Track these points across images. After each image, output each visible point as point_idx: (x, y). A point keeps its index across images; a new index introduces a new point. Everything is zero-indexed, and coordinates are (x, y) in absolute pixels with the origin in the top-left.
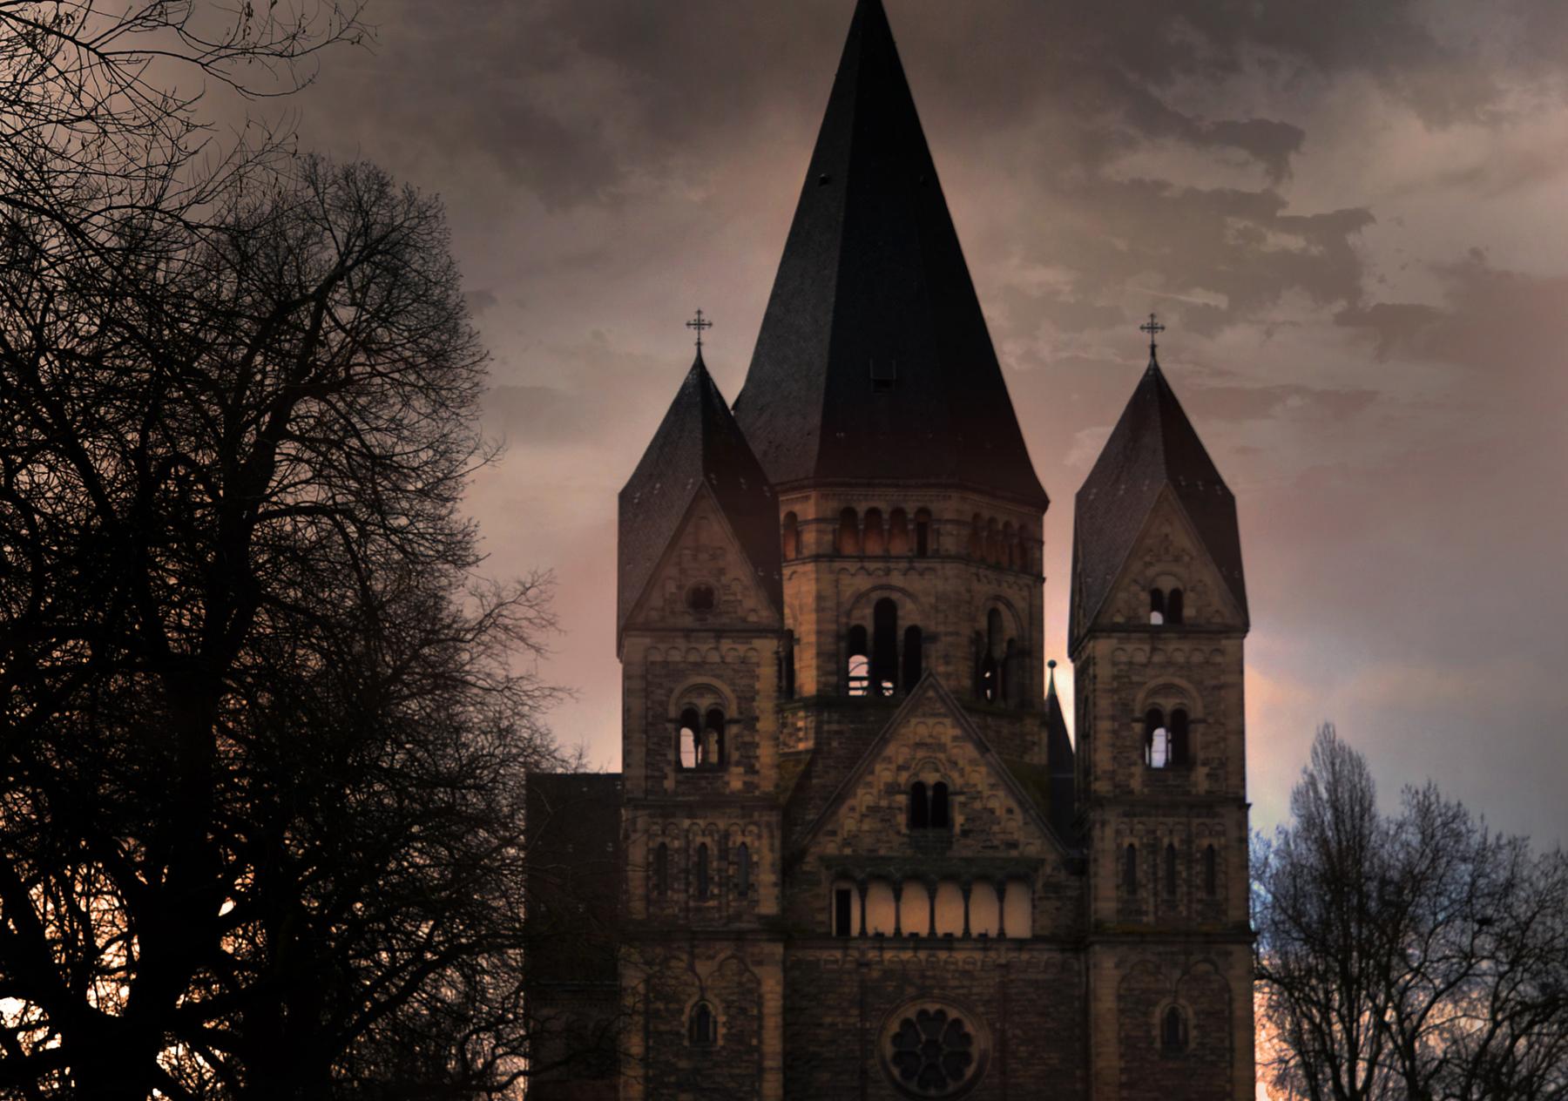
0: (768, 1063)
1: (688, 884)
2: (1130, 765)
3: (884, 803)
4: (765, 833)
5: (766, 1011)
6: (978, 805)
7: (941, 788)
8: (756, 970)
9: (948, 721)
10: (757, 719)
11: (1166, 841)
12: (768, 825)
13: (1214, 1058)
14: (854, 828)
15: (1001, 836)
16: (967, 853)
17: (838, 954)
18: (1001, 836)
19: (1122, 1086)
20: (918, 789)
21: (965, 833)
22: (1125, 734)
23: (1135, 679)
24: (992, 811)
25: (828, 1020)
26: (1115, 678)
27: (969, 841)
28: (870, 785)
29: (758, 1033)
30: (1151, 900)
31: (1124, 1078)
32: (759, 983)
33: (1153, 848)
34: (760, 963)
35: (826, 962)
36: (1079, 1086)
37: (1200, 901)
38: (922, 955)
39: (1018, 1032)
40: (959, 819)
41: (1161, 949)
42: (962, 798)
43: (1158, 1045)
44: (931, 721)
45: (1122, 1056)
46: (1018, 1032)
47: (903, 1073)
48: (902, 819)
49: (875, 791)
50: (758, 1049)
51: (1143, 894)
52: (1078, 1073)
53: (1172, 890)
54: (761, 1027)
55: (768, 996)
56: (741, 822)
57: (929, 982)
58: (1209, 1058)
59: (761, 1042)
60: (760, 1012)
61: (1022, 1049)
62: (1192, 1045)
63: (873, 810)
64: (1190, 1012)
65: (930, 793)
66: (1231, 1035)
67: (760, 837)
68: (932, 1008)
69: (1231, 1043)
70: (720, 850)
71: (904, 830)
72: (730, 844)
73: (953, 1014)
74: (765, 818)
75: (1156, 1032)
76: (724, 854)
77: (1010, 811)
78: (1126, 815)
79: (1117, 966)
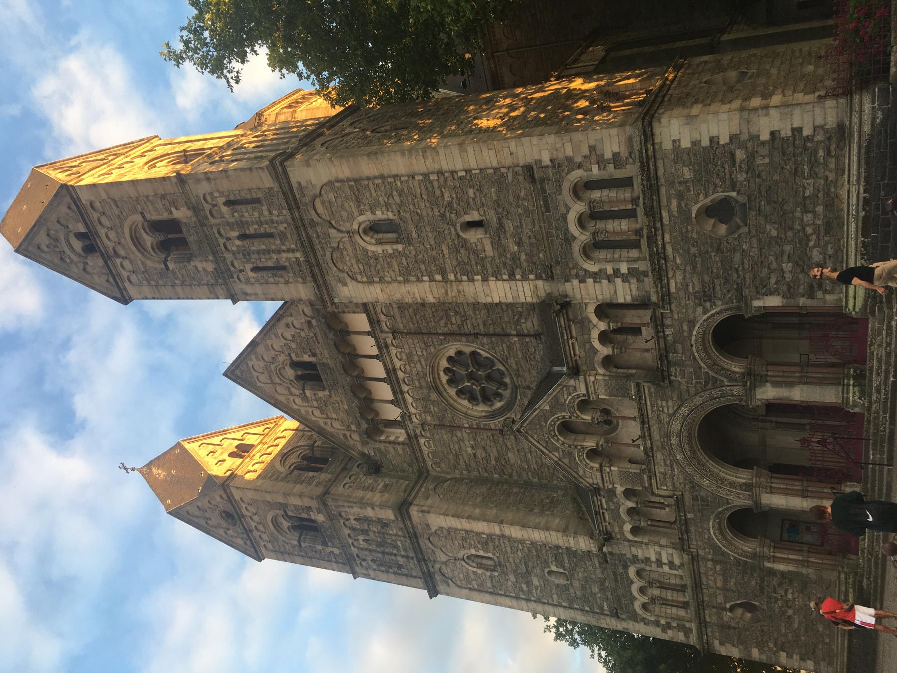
1: (391, 554)
11: (238, 242)
16: (327, 355)
19: (445, 280)
21: (314, 355)
27: (318, 352)
31: (438, 277)
38: (405, 388)
39: (442, 323)
41: (318, 247)
42: (293, 355)
43: (400, 247)
45: (419, 280)
48: (321, 394)
57: (424, 384)
58: (397, 199)
61: (454, 320)
62: (390, 215)
65: (299, 373)
66: (368, 179)
68: (444, 378)
71: (327, 393)
73: (444, 364)
75: (389, 249)
79: (345, 284)
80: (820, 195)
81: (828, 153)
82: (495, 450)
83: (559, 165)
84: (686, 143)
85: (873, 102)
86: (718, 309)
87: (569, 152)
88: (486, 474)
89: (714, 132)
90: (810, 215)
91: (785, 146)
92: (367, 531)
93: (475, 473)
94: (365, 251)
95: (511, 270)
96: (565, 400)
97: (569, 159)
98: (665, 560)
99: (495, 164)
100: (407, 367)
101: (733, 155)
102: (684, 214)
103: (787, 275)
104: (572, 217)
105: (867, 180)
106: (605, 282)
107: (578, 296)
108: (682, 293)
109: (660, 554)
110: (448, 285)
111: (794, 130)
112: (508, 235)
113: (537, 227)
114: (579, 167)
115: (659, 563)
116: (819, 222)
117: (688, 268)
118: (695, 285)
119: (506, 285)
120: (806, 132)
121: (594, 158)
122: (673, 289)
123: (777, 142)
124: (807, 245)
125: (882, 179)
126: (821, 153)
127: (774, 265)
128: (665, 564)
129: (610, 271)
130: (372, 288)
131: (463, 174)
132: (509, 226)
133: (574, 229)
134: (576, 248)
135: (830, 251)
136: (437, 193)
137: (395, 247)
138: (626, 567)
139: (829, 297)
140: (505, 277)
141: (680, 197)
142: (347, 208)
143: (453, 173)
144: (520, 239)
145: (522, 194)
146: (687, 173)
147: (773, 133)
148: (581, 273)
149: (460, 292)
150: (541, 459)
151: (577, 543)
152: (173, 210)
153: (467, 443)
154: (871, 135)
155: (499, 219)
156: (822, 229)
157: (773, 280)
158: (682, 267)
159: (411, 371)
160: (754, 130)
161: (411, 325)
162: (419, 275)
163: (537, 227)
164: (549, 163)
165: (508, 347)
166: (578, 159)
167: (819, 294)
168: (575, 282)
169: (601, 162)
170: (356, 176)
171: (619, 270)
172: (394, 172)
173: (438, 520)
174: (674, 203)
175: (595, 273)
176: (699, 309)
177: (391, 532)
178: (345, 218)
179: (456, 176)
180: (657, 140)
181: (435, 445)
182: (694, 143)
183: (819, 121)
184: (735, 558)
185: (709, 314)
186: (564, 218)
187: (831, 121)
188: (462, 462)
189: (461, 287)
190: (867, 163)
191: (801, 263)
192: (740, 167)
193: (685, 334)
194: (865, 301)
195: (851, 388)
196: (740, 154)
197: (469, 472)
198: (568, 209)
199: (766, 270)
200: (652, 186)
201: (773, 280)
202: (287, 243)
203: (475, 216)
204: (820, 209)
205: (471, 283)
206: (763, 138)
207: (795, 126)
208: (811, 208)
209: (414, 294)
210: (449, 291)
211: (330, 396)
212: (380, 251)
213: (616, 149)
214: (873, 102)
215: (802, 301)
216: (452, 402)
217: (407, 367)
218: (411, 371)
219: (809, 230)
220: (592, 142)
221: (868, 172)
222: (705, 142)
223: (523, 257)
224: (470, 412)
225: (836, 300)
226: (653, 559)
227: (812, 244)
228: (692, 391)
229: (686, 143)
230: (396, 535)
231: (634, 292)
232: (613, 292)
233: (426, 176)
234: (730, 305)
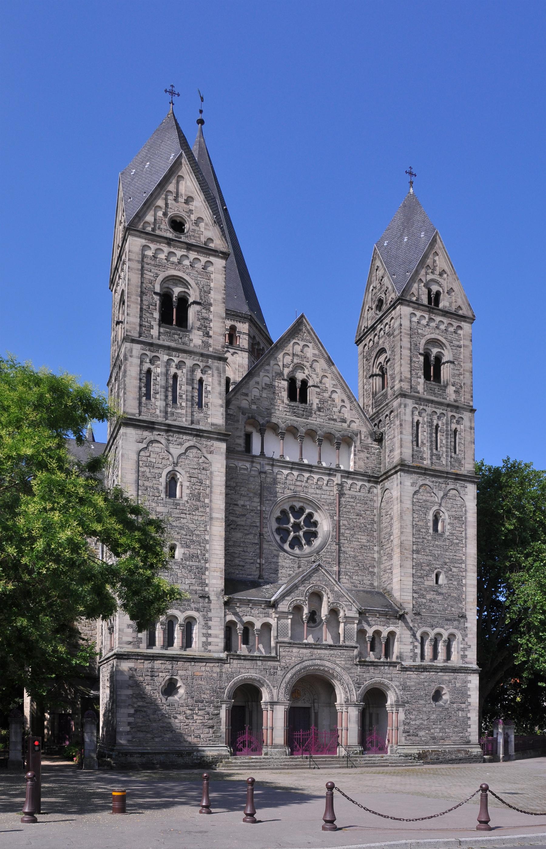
17: (248, 465)
25: (241, 502)
35: (241, 469)
82: (243, 523)
84: (469, 685)
89: (472, 697)
97: (466, 636)
98: (210, 640)
101: (464, 703)
104: (441, 631)
109: (216, 637)
111: (470, 725)
112: (435, 596)
113: (438, 612)
114: (463, 640)
115: (210, 635)
121: (466, 646)
128: (207, 639)
132: (440, 598)
133: (437, 630)
134: (428, 630)
138: (197, 610)
141: (450, 682)
144: (432, 602)
145: (453, 609)
147: (470, 718)
150: (239, 557)
153: (248, 503)
160: (471, 711)
163: (438, 612)
166: (466, 639)
169: (464, 649)
171: (417, 648)
180: (471, 675)
181: (243, 474)
182: (469, 688)
183: (472, 734)
184: (226, 687)
186: (443, 627)
187: (471, 738)
196: (463, 706)
198: (446, 630)
200: (455, 670)
206: (468, 714)
222: (469, 693)
226: (210, 632)
229: (469, 685)
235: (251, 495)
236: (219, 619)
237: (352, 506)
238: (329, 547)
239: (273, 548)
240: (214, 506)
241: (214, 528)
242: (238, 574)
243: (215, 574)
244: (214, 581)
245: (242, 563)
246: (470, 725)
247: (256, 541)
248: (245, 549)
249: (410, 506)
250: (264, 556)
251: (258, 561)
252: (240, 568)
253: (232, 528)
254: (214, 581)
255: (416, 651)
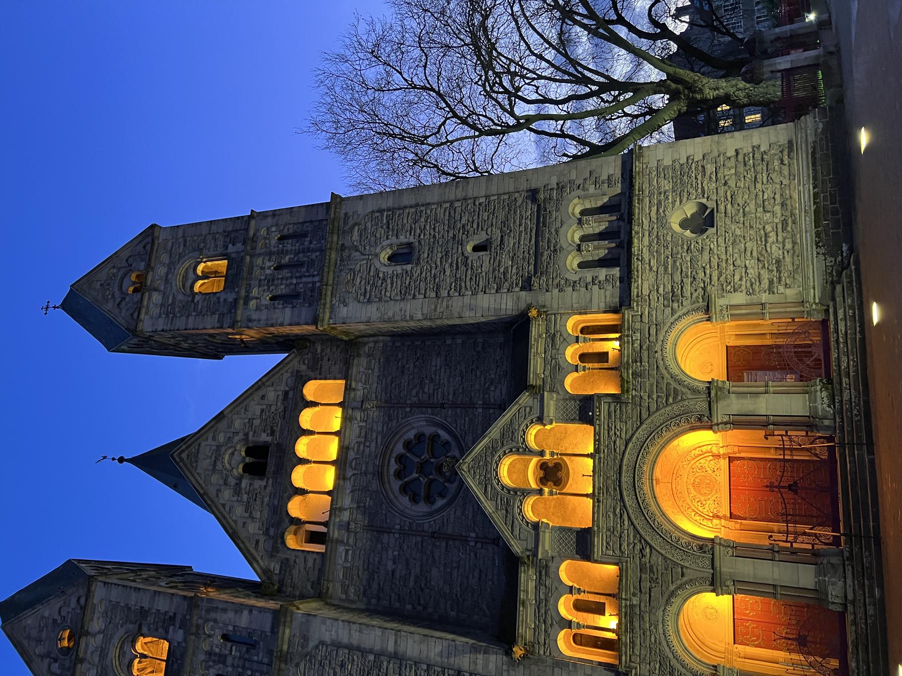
0: (391, 648)
2: (219, 302)
3: (245, 497)
4: (213, 615)
5: (345, 640)
6: (257, 422)
7: (249, 452)
8: (312, 644)
9: (203, 444)
10: (142, 608)
12: (208, 611)
13: (423, 220)
14: (257, 525)
15: (279, 404)
17: (341, 549)
18: (279, 404)
20: (247, 469)
21: (272, 433)
22: (200, 307)
23: (170, 301)
24: (262, 411)
25: (390, 565)
26: (167, 316)
28: (231, 508)
29: (364, 652)
30: (304, 280)
31: (433, 295)
32: (322, 643)
33: (271, 281)
34: (306, 639)
36: (459, 341)
37: (311, 243)
40: (264, 437)
42: (251, 434)
44: (201, 456)
45: (414, 297)
46: (414, 392)
47: (442, 495)
49: (236, 504)
50: (378, 655)
51: (301, 289)
52: (449, 342)
53: (302, 264)
54: (358, 649)
55: (334, 637)
56: (203, 636)
59: (371, 651)
60: (346, 647)
62: (412, 239)
63: (248, 508)
64: (388, 242)
66: (406, 207)
67: (215, 621)
69: (411, 207)
70: (219, 662)
72: (217, 650)
73: (399, 449)
74: (203, 612)
75: (399, 269)
76: (222, 659)
77: (263, 397)
78: (246, 303)
80: (777, 196)
81: (782, 163)
83: (563, 187)
85: (815, 118)
86: (685, 310)
87: (573, 176)
88: (397, 605)
89: (690, 151)
90: (768, 215)
91: (746, 159)
92: (226, 656)
93: (385, 603)
94: (377, 271)
95: (499, 284)
96: (519, 426)
99: (512, 189)
100: (362, 447)
101: (703, 167)
102: (662, 221)
103: (750, 271)
105: (815, 178)
106: (584, 289)
107: (555, 306)
108: (654, 295)
110: (440, 301)
111: (753, 147)
116: (777, 221)
117: (661, 269)
118: (665, 286)
119: (492, 298)
120: (762, 149)
122: (646, 292)
123: (740, 157)
124: (766, 241)
125: (829, 174)
126: (776, 163)
127: (738, 263)
129: (589, 279)
130: (369, 307)
131: (482, 200)
132: (510, 242)
135: (789, 246)
136: (458, 217)
137: (404, 267)
139: (789, 292)
140: (493, 291)
142: (378, 235)
143: (475, 199)
146: (667, 185)
147: (736, 151)
148: (563, 282)
149: (447, 307)
151: (486, 665)
152: (230, 245)
153: (390, 553)
154: (815, 142)
155: (502, 236)
156: (780, 226)
157: (737, 277)
158: (655, 269)
159: (363, 451)
160: (722, 149)
161: (384, 395)
162: (417, 293)
164: (555, 186)
165: (470, 420)
167: (781, 289)
168: (556, 291)
170: (396, 206)
172: (427, 201)
173: (323, 628)
174: (654, 209)
175: (575, 282)
176: (668, 311)
177: (255, 658)
178: (372, 243)
179: (477, 203)
182: (674, 161)
183: (773, 139)
185: (676, 316)
187: (783, 140)
188: (375, 586)
189: (450, 303)
190: (814, 164)
191: (762, 259)
192: (710, 177)
193: (652, 339)
194: (824, 288)
195: (819, 393)
196: (710, 168)
197: (379, 599)
199: (732, 267)
201: (737, 277)
202: (312, 270)
203: (481, 238)
204: (778, 208)
205: (461, 298)
206: (728, 155)
207: (754, 144)
208: (769, 207)
209: (405, 311)
210: (439, 306)
211: (265, 487)
212: (390, 272)
213: (611, 172)
214: (815, 118)
215: (765, 297)
216: (392, 496)
217: (362, 447)
218: (363, 451)
219: (769, 228)
220: (593, 167)
221: (815, 171)
223: (514, 270)
224: (407, 511)
225: (797, 294)
227: (770, 240)
228: (653, 407)
229: (667, 162)
230: (261, 663)
231: (608, 299)
232: (588, 299)
233: (452, 203)
234: (697, 305)
235: (379, 546)
236: (556, 669)
237: (392, 382)
238: (449, 420)
239: (452, 517)
240: (377, 647)
241: (409, 653)
242: (493, 583)
243: (480, 662)
244: (492, 666)
245: (476, 575)
246: (753, 147)
247: (444, 544)
248: (455, 565)
249: (375, 305)
250: (464, 534)
251: (472, 544)
252: (483, 577)
253: (426, 584)
254: (492, 666)
255: (602, 277)
